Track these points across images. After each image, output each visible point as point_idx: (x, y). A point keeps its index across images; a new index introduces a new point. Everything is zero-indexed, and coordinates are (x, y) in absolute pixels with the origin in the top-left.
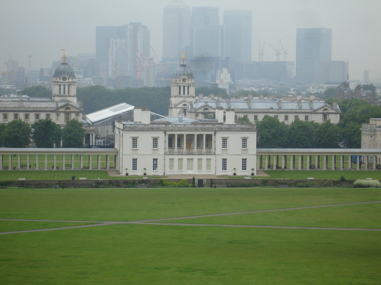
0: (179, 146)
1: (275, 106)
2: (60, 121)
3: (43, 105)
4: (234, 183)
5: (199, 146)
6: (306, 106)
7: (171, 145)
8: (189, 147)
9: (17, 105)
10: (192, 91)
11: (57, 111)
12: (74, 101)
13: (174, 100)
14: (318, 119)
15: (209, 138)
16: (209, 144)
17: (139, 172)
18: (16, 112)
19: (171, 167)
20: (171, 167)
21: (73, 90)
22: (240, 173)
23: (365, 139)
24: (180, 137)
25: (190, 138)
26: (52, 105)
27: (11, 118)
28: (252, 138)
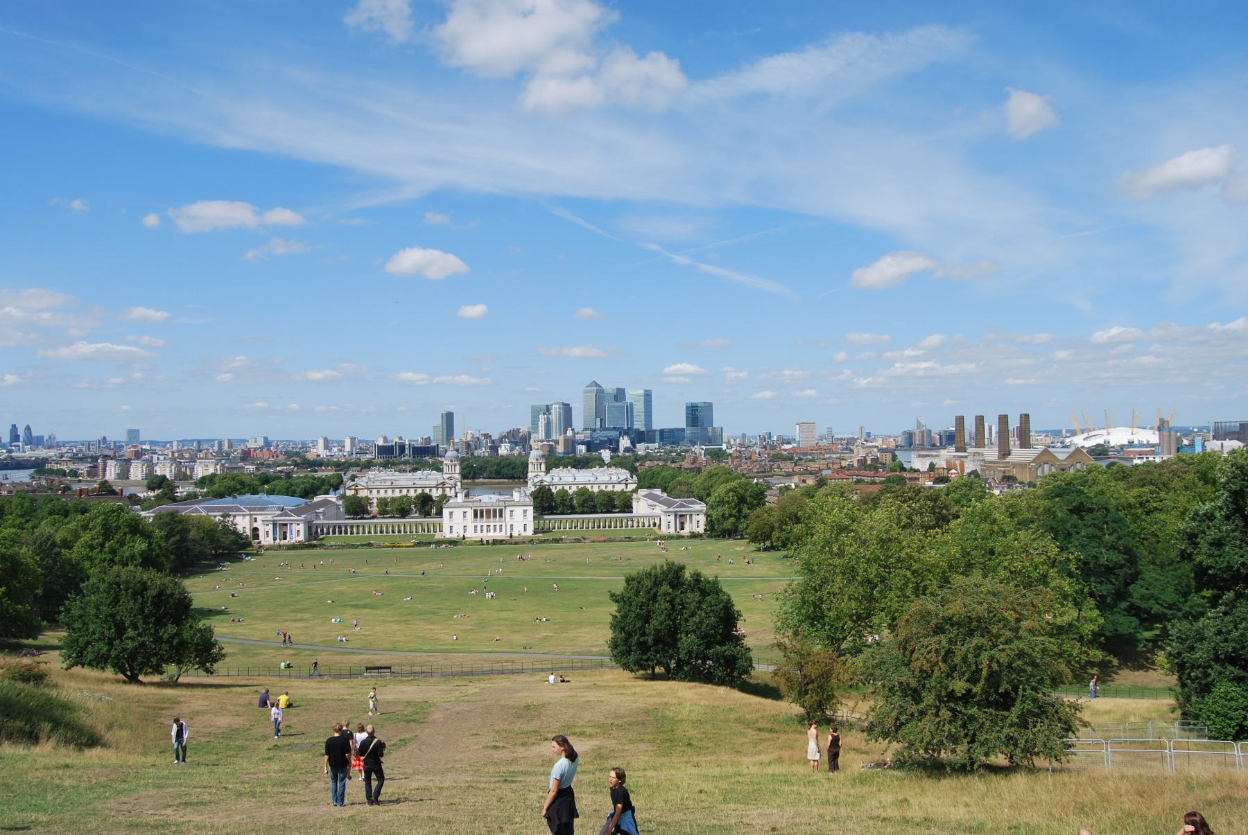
0: (482, 516)
1: (592, 479)
2: (435, 494)
3: (427, 483)
4: (512, 542)
5: (495, 516)
6: (614, 478)
7: (476, 516)
8: (488, 517)
9: (410, 483)
10: (543, 466)
11: (437, 487)
12: (458, 476)
13: (530, 475)
14: (618, 488)
15: (501, 511)
16: (501, 516)
17: (454, 535)
18: (408, 488)
19: (476, 530)
20: (476, 530)
21: (458, 469)
22: (524, 534)
23: (634, 504)
24: (482, 512)
25: (488, 512)
26: (435, 483)
27: (404, 492)
28: (531, 510)
